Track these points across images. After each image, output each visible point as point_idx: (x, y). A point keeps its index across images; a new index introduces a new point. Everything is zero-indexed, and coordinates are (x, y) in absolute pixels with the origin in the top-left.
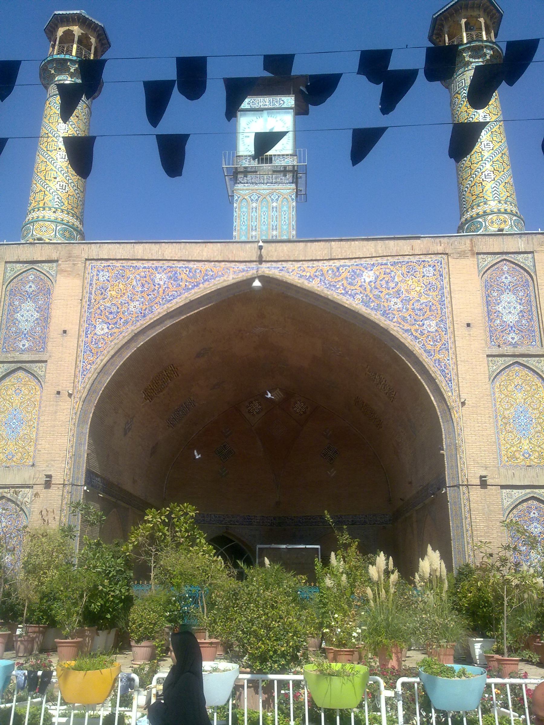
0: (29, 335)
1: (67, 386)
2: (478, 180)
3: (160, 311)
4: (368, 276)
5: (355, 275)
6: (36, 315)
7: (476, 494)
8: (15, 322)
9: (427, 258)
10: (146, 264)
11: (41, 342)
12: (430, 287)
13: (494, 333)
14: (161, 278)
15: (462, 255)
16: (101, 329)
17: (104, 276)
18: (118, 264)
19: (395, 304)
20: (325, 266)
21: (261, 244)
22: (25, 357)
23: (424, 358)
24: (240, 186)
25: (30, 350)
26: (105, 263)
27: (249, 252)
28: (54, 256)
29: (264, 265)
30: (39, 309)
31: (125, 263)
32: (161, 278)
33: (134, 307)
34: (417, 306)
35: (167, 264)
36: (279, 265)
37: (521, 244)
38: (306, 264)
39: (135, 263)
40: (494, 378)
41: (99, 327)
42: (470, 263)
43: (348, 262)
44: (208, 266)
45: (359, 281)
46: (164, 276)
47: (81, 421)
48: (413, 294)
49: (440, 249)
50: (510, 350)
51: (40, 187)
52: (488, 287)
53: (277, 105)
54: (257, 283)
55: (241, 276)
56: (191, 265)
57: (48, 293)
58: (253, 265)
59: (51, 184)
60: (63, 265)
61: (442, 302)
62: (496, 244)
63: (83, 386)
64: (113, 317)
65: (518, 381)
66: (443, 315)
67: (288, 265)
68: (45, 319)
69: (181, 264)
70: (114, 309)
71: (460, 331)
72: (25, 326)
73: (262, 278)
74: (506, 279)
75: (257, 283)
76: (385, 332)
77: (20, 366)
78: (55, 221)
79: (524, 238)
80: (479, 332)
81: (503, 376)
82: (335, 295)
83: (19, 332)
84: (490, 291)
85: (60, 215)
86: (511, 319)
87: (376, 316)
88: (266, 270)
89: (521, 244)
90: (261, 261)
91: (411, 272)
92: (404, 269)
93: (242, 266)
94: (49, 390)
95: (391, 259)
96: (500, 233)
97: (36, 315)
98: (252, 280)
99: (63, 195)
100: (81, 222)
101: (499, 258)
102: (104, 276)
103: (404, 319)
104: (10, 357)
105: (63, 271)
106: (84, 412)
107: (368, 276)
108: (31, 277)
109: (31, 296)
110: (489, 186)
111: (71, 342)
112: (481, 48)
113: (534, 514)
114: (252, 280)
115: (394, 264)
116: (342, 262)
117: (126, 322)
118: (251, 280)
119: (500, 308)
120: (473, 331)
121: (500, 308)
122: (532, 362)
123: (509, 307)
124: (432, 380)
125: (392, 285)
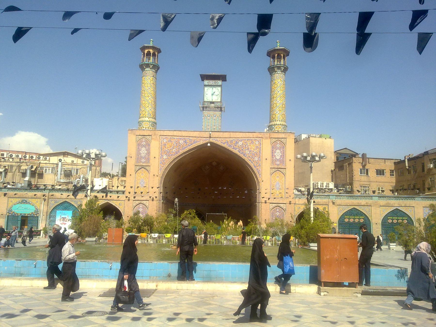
0: (144, 158)
1: (156, 174)
2: (274, 113)
3: (181, 152)
4: (240, 143)
5: (237, 143)
6: (146, 152)
7: (263, 205)
8: (140, 154)
9: (257, 139)
10: (177, 137)
11: (148, 160)
12: (257, 147)
13: (273, 162)
14: (181, 142)
15: (266, 138)
16: (165, 157)
17: (165, 141)
18: (169, 137)
19: (247, 152)
20: (228, 140)
21: (210, 133)
22: (144, 165)
23: (254, 168)
24: (204, 111)
25: (145, 162)
26: (165, 137)
27: (207, 135)
28: (150, 134)
29: (211, 139)
30: (147, 150)
31: (171, 137)
32: (181, 142)
33: (174, 150)
34: (253, 153)
35: (183, 138)
36: (215, 139)
37: (283, 136)
38: (223, 139)
39: (174, 137)
40: (271, 174)
41: (164, 156)
42: (268, 141)
43: (235, 139)
44: (195, 138)
45: (238, 145)
46: (182, 141)
47: (161, 183)
48: (252, 149)
49: (261, 136)
50: (276, 167)
51: (143, 110)
52: (273, 148)
53: (216, 84)
54: (209, 145)
55: (204, 142)
56: (190, 138)
57: (149, 145)
58: (208, 139)
59: (147, 109)
60: (153, 137)
61: (260, 152)
62: (276, 135)
63: (161, 173)
64: (168, 153)
65: (278, 175)
66: (260, 156)
67: (218, 139)
68: (149, 153)
69: (187, 138)
70: (168, 151)
71: (264, 160)
72: (143, 155)
73: (211, 143)
74: (278, 146)
75: (209, 145)
76: (244, 160)
77: (143, 167)
78: (149, 122)
79: (284, 134)
80: (269, 161)
81: (274, 174)
82: (231, 149)
83: (141, 157)
84: (274, 148)
85: (150, 119)
86: (278, 158)
87: (242, 156)
88: (211, 140)
89: (283, 136)
90: (210, 138)
91: (252, 142)
92: (250, 142)
93: (205, 139)
94: (151, 174)
95: (247, 139)
96: (278, 132)
97: (146, 152)
98: (208, 143)
99: (151, 112)
100: (155, 119)
101: (277, 139)
102: (165, 141)
103: (249, 156)
104: (140, 164)
105: (153, 139)
106: (161, 180)
107: (240, 143)
108: (144, 140)
109: (143, 146)
110: (277, 115)
111: (157, 160)
112: (280, 67)
113: (278, 210)
114: (208, 143)
115: (248, 140)
116: (233, 139)
117: (172, 155)
118: (207, 143)
119: (275, 154)
120: (267, 160)
121: (275, 154)
122: (282, 170)
123: (278, 154)
124: (255, 174)
125: (247, 146)
